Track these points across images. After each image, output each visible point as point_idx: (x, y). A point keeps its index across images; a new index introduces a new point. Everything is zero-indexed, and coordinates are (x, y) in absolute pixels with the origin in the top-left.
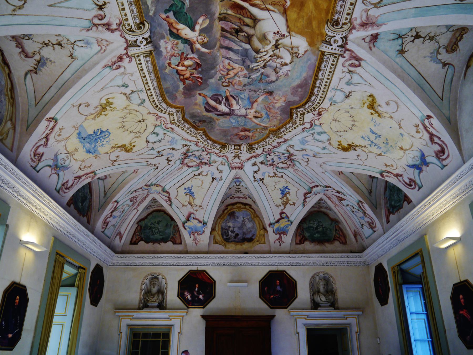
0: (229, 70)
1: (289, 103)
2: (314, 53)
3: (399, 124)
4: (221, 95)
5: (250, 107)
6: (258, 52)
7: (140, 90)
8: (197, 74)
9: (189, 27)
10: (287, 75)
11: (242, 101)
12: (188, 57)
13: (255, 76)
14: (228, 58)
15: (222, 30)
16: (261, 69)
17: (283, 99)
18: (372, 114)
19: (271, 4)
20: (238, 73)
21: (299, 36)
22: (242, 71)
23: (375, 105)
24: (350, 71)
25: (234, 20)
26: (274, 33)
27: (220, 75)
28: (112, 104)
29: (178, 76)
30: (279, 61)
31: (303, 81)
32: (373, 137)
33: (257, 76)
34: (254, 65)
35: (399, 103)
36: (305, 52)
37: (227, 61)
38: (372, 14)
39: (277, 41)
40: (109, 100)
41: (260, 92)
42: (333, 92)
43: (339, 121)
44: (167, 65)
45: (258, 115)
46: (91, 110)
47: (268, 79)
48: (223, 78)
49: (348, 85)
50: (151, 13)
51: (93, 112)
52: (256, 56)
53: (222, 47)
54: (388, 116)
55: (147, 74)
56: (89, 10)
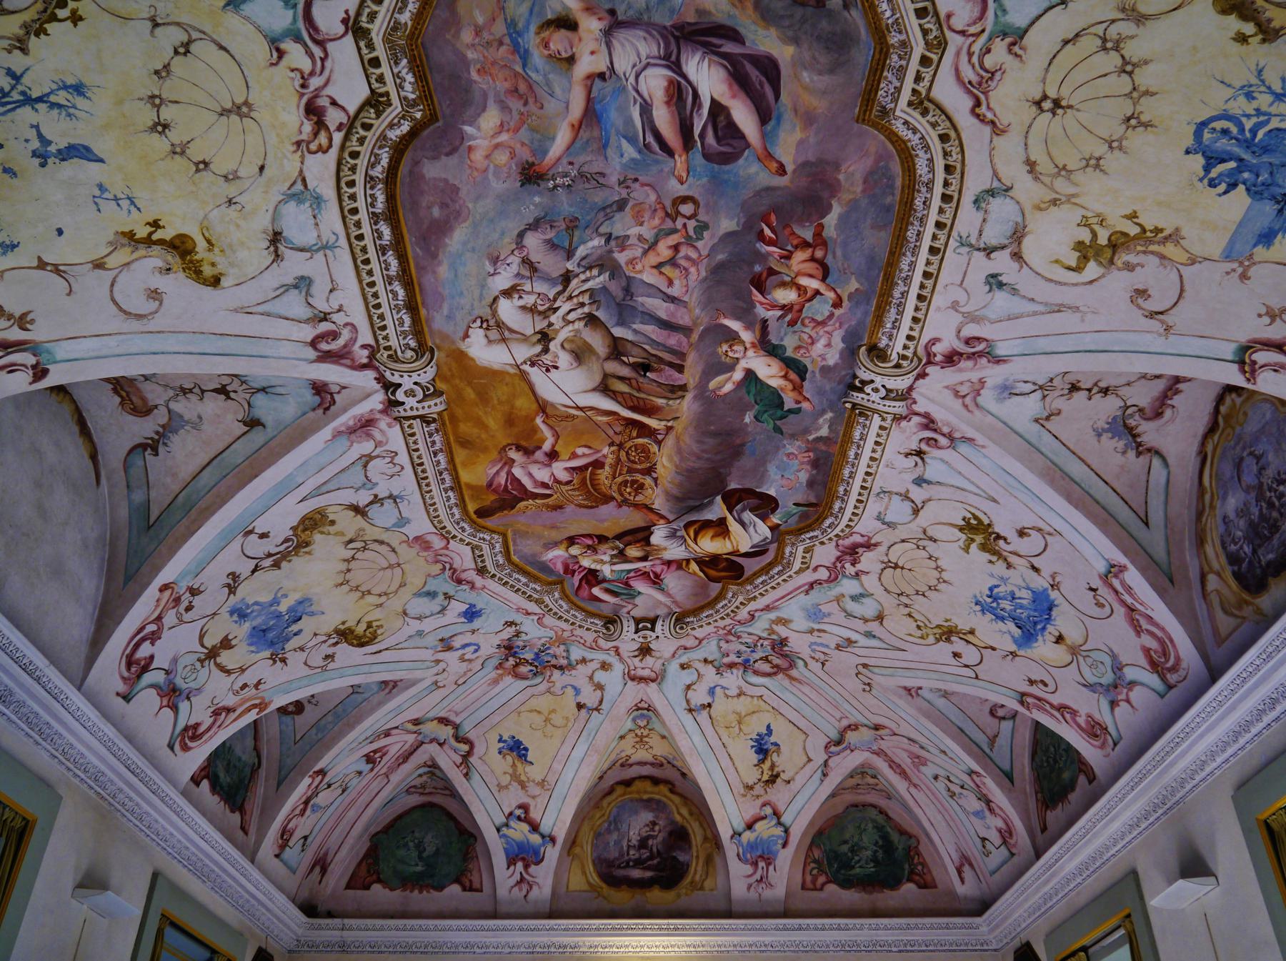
0: (672, 262)
1: (453, 144)
2: (445, 337)
3: (57, 270)
4: (707, 156)
5: (598, 82)
6: (591, 320)
7: (965, 250)
8: (769, 254)
9: (757, 378)
10: (495, 260)
11: (629, 121)
12: (780, 313)
13: (591, 246)
14: (672, 299)
15: (683, 366)
16: (577, 270)
17: (478, 156)
18: (156, 224)
19: (574, 417)
20: (645, 252)
21: (496, 367)
22: (631, 262)
23: (178, 259)
24: (326, 320)
25: (654, 387)
26: (556, 368)
27: (699, 244)
28: (1079, 246)
29: (829, 260)
30: (529, 300)
31: (437, 249)
32: (59, 131)
33: (584, 242)
34: (599, 280)
35: (135, 325)
36: (466, 336)
37: (676, 291)
38: (365, 444)
39: (546, 350)
40: (1073, 264)
41: (566, 175)
42: (327, 236)
43: (225, 112)
44: (846, 303)
45: (559, 41)
46: (1150, 272)
47: (550, 235)
48: (691, 233)
49: (302, 278)
50: (829, 415)
51: (1153, 261)
52: (595, 307)
53: (687, 331)
54: (112, 262)
55: (912, 301)
56: (942, 460)
